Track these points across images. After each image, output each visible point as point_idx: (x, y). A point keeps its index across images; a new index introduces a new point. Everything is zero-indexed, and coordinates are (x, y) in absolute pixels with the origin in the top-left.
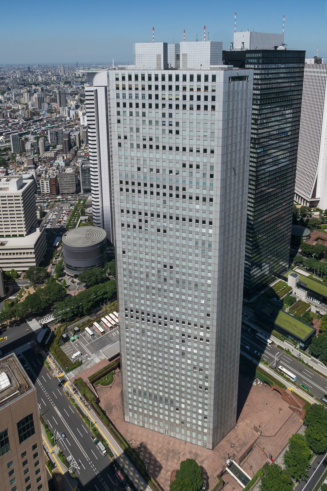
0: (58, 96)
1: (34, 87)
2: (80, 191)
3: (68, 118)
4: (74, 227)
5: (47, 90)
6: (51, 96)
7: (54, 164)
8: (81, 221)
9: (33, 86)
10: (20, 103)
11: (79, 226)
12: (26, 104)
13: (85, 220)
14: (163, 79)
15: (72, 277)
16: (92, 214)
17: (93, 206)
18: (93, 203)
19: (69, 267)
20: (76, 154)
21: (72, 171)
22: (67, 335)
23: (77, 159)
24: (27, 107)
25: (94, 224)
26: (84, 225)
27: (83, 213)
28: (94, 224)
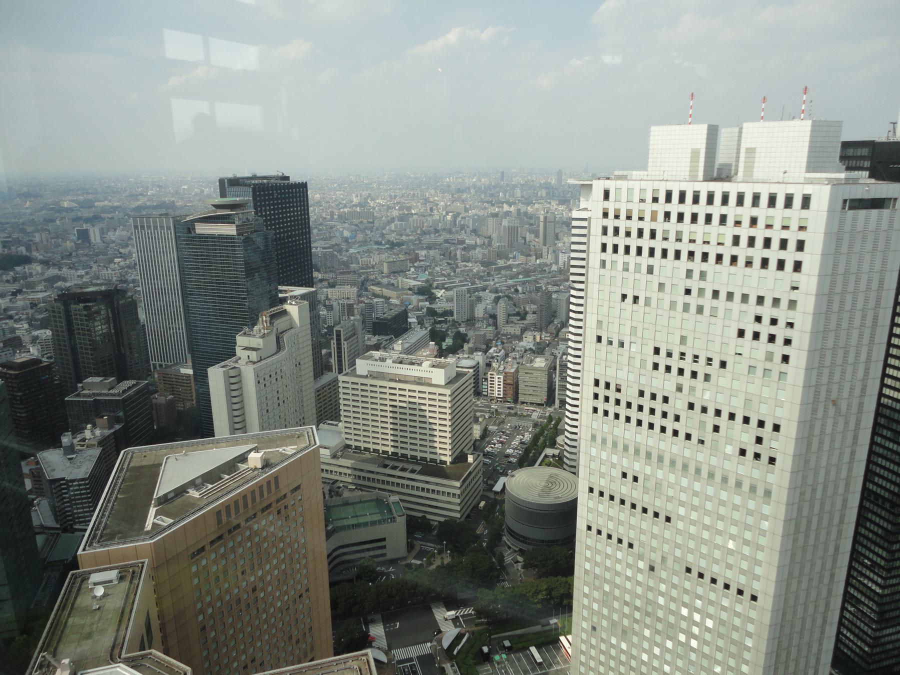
0: (542, 224)
1: (506, 208)
2: (554, 402)
3: (554, 268)
4: (533, 465)
5: (526, 214)
6: (531, 225)
7: (517, 349)
8: (546, 456)
9: (505, 205)
10: (479, 236)
11: (540, 465)
12: (490, 237)
13: (554, 456)
14: (710, 200)
15: (515, 551)
16: (563, 446)
17: (566, 433)
18: (567, 427)
19: (513, 534)
20: (557, 335)
21: (543, 365)
22: (490, 650)
23: (558, 342)
24: (490, 245)
25: (565, 466)
26: (549, 465)
27: (553, 444)
28: (565, 466)
